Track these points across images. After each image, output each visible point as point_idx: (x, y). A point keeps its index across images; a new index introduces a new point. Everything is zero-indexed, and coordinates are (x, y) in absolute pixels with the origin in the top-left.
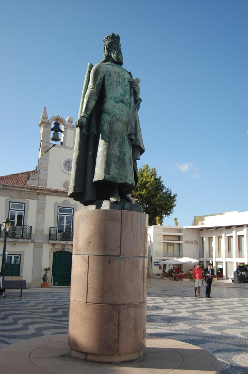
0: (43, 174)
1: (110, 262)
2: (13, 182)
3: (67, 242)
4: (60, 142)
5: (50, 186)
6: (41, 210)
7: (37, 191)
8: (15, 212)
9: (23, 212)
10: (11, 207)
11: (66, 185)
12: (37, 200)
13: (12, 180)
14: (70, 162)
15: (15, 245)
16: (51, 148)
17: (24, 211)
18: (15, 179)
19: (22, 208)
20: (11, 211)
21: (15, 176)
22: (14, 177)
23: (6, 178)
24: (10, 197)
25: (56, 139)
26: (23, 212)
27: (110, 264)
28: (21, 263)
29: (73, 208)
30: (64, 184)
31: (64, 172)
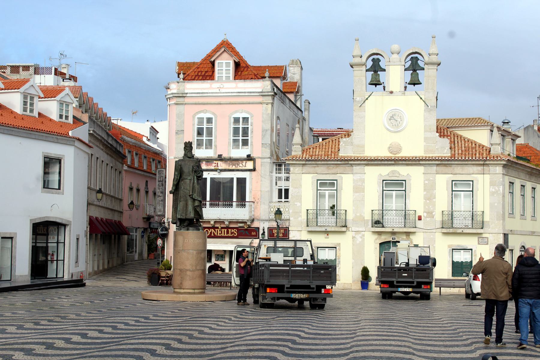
0: (359, 136)
3: (393, 230)
4: (382, 86)
5: (370, 153)
6: (359, 189)
7: (349, 163)
9: (336, 191)
10: (320, 187)
11: (391, 149)
12: (352, 173)
14: (397, 114)
16: (367, 99)
17: (337, 190)
19: (334, 187)
20: (319, 192)
24: (317, 173)
25: (376, 83)
26: (336, 191)
28: (337, 258)
29: (405, 181)
30: (389, 148)
31: (388, 129)
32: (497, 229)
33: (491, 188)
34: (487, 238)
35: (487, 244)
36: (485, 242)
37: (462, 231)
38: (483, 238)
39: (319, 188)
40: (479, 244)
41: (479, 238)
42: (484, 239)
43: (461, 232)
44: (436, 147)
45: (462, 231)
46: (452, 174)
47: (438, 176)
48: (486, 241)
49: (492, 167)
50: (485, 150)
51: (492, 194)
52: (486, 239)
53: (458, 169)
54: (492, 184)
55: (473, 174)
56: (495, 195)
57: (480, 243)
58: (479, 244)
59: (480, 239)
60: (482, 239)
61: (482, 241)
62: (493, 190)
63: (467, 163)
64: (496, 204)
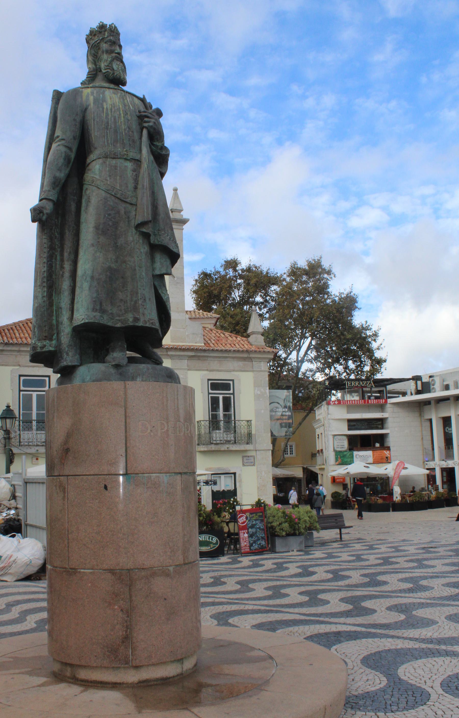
1: (106, 487)
2: (22, 335)
8: (32, 395)
13: (21, 331)
15: (37, 459)
18: (28, 329)
21: (27, 323)
22: (26, 325)
23: (8, 330)
24: (19, 365)
27: (107, 492)
32: (265, 445)
33: (256, 390)
34: (253, 457)
35: (254, 465)
36: (251, 463)
37: (228, 448)
38: (248, 457)
39: (22, 388)
40: (244, 465)
41: (243, 457)
42: (250, 458)
43: (226, 449)
44: (187, 334)
45: (228, 448)
46: (207, 370)
47: (189, 372)
48: (252, 460)
49: (256, 363)
50: (241, 341)
51: (257, 397)
52: (252, 458)
53: (215, 364)
54: (256, 385)
55: (234, 371)
56: (261, 399)
57: (245, 464)
58: (244, 465)
59: (245, 458)
60: (247, 458)
61: (248, 461)
62: (259, 393)
63: (224, 355)
64: (263, 411)
